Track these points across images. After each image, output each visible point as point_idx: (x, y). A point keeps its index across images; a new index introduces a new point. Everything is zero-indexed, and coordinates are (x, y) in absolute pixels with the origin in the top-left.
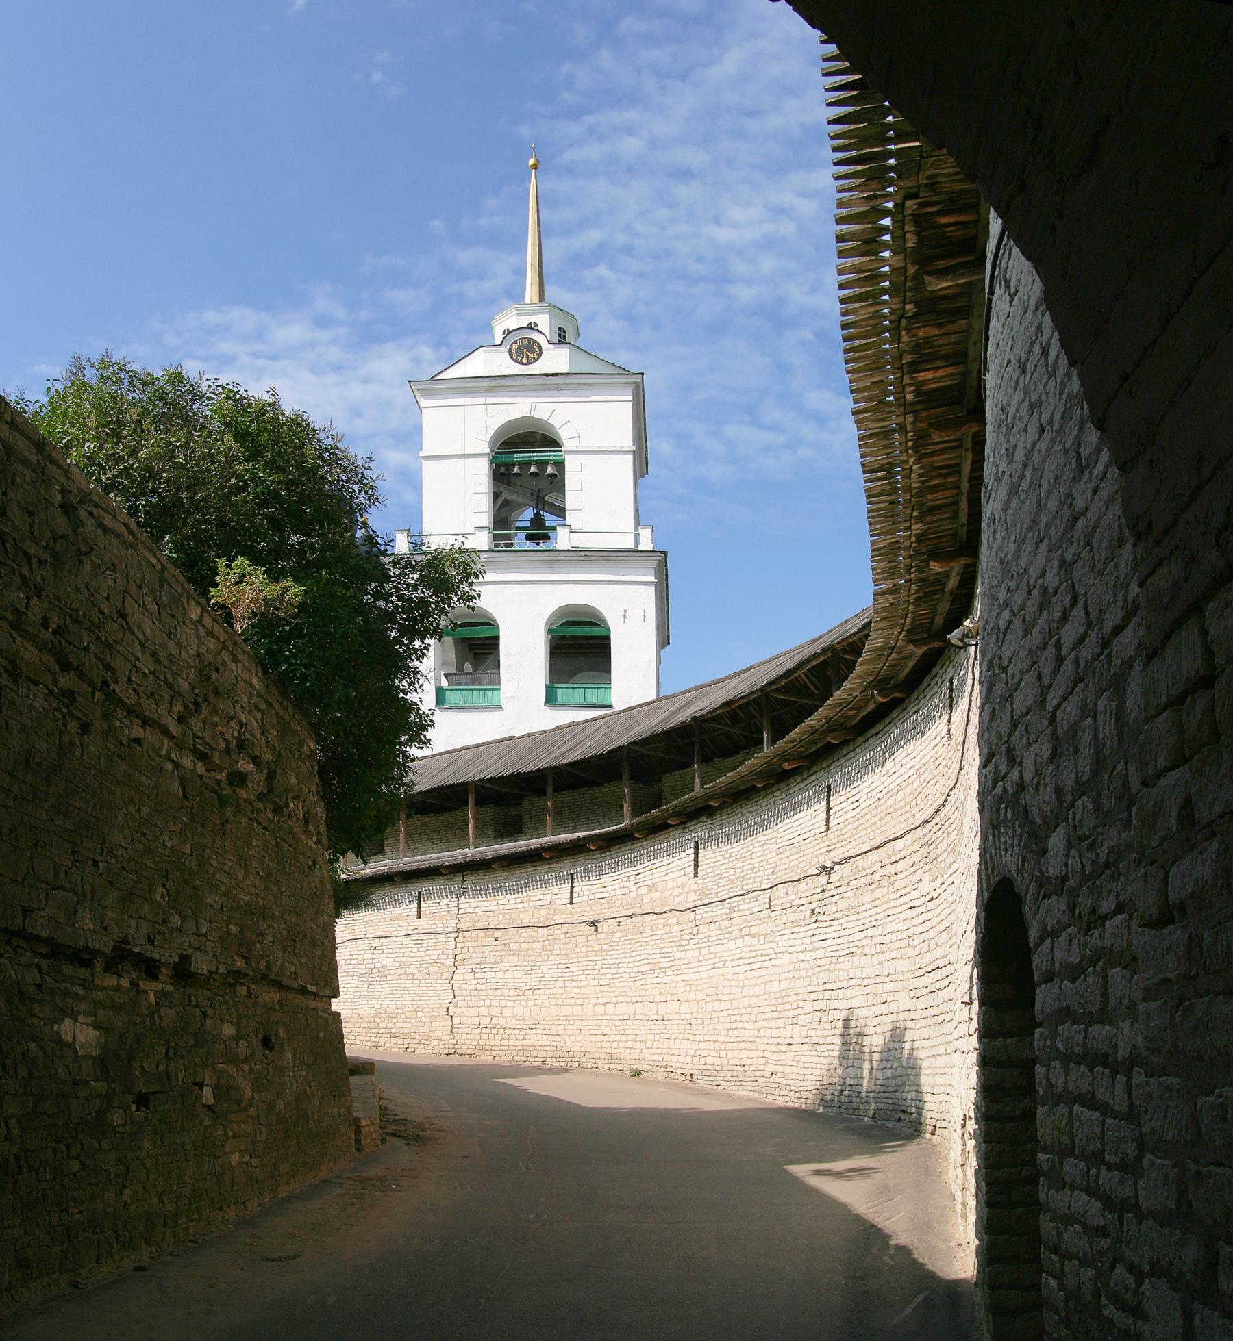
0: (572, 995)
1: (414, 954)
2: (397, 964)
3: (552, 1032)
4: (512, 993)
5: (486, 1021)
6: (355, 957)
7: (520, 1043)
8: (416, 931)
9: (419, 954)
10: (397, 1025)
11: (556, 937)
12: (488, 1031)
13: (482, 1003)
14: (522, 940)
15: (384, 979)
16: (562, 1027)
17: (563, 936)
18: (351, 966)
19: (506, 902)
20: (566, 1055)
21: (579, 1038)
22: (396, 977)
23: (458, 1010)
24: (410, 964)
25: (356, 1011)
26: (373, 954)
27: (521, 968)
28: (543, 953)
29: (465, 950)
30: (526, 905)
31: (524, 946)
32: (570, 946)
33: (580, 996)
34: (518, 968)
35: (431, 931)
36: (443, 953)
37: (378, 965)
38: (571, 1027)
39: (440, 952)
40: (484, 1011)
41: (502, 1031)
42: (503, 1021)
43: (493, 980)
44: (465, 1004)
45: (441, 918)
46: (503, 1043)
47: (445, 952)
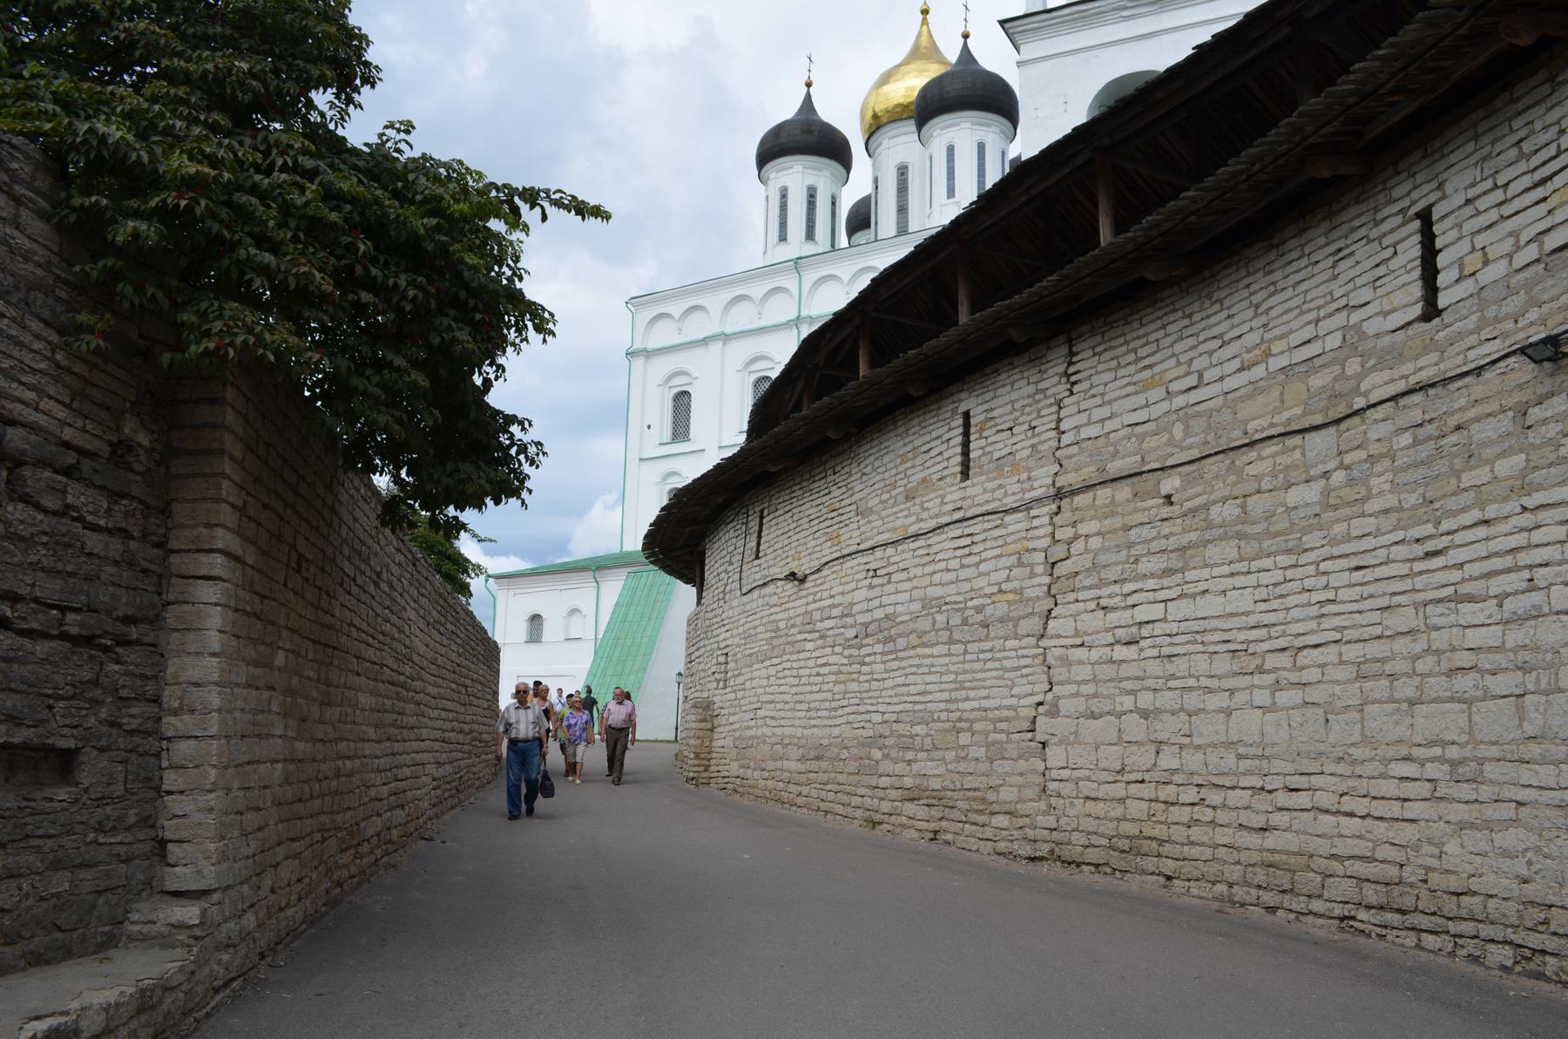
0: (1465, 659)
1: (951, 576)
2: (916, 606)
3: (1379, 808)
4: (1222, 664)
5: (1142, 758)
6: (838, 600)
7: (1253, 840)
8: (958, 515)
9: (964, 574)
10: (915, 767)
11: (1375, 449)
12: (1147, 791)
13: (1128, 702)
14: (1250, 487)
15: (890, 646)
16: (1424, 789)
17: (1406, 439)
18: (829, 623)
19: (1192, 380)
20: (1449, 906)
21: (1511, 838)
22: (913, 639)
23: (1062, 725)
24: (941, 604)
25: (836, 731)
26: (871, 587)
27: (1251, 580)
28: (1328, 516)
29: (1078, 546)
30: (1259, 372)
31: (1257, 505)
32: (1442, 466)
33: (1501, 659)
34: (1239, 581)
35: (989, 507)
36: (1020, 564)
37: (879, 614)
38: (1465, 791)
39: (1013, 559)
40: (1135, 728)
41: (1190, 795)
42: (1193, 760)
43: (1158, 629)
44: (1078, 705)
45: (1016, 468)
46: (1196, 833)
47: (1027, 558)
